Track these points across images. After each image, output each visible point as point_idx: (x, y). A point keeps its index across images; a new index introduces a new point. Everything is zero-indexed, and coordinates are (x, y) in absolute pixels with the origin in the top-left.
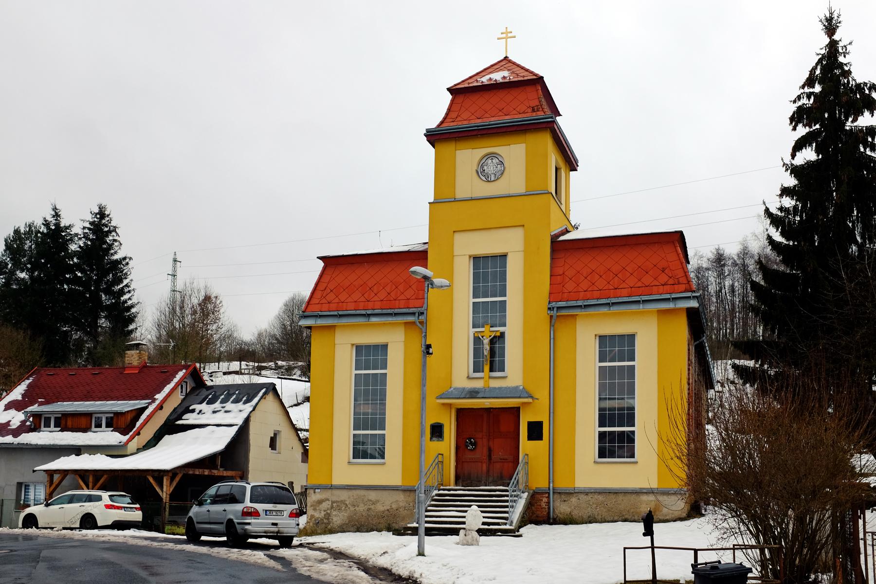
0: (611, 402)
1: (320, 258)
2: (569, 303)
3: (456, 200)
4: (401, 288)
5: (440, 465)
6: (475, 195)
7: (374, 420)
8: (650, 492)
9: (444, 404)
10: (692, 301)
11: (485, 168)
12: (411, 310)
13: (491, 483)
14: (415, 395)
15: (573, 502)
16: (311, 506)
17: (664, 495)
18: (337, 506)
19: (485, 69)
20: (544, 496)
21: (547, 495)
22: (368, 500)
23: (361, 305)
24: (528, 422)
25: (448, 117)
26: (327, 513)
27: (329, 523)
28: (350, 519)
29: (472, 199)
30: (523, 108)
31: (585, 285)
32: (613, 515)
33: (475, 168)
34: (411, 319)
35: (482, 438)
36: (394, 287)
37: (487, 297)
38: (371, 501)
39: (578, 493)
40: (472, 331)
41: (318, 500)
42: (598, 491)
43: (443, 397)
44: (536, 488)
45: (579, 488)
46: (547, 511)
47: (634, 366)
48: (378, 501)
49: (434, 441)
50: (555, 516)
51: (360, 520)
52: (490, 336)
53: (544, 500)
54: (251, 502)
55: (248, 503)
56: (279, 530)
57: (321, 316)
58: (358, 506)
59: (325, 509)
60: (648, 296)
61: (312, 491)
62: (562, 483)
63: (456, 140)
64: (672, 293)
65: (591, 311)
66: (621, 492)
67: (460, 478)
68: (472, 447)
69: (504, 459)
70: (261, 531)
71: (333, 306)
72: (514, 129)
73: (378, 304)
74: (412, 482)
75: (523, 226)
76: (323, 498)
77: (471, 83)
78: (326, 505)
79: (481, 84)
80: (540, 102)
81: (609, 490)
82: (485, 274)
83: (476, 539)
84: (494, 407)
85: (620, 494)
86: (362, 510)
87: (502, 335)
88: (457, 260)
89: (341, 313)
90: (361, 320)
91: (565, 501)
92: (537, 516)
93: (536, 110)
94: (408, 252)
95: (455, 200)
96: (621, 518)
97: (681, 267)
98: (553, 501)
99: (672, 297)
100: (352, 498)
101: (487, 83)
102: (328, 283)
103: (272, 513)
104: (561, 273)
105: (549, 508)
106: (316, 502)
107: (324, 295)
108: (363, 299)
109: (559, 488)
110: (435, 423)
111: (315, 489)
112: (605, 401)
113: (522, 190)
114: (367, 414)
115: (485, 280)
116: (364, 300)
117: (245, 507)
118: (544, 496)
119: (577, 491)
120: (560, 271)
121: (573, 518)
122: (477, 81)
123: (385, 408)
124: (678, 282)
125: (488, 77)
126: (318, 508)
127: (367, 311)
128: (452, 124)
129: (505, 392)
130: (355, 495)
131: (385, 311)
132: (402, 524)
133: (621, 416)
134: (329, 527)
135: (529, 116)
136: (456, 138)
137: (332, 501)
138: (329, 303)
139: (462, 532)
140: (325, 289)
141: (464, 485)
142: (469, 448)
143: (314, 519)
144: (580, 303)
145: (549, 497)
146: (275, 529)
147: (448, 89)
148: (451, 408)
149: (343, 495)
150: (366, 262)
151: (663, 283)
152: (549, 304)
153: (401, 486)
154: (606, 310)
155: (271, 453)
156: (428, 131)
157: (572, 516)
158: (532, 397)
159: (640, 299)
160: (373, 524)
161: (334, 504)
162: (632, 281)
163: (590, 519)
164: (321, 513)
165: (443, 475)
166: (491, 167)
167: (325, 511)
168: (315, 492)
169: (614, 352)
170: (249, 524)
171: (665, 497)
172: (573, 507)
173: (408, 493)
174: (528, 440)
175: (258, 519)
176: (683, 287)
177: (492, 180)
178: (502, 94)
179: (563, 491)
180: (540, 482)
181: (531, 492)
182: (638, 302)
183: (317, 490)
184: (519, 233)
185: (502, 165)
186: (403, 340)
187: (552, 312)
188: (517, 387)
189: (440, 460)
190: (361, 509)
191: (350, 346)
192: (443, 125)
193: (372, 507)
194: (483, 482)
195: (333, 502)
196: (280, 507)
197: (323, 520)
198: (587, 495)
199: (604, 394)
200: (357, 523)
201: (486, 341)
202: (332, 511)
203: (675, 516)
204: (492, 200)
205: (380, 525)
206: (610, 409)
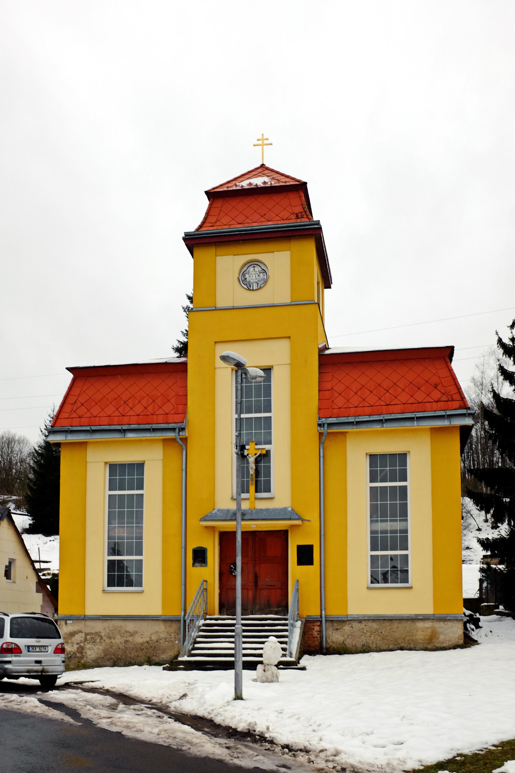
1: (70, 369)
2: (340, 419)
3: (217, 308)
4: (159, 402)
5: (205, 593)
6: (237, 304)
7: (130, 544)
8: (425, 618)
9: (206, 527)
10: (467, 418)
11: (247, 276)
12: (171, 426)
13: (257, 611)
14: (176, 517)
15: (346, 630)
17: (440, 621)
18: (92, 638)
19: (249, 172)
20: (316, 624)
21: (319, 624)
22: (125, 631)
23: (116, 419)
24: (297, 546)
25: (207, 221)
26: (81, 646)
27: (82, 657)
28: (106, 652)
29: (233, 308)
30: (285, 214)
31: (355, 400)
32: (388, 643)
33: (237, 276)
34: (170, 435)
35: (247, 564)
36: (151, 401)
38: (128, 632)
39: (351, 620)
41: (70, 633)
42: (372, 618)
43: (207, 519)
44: (307, 616)
45: (352, 615)
46: (319, 641)
47: (406, 486)
48: (136, 633)
49: (196, 566)
50: (328, 646)
51: (117, 653)
52: (255, 454)
53: (315, 629)
54: (12, 636)
55: (7, 637)
56: (43, 669)
57: (72, 432)
58: (114, 638)
59: (77, 642)
60: (422, 413)
61: (63, 623)
62: (333, 611)
63: (216, 246)
64: (446, 410)
65: (363, 428)
66: (396, 619)
67: (224, 607)
69: (271, 586)
70: (23, 670)
71: (84, 420)
72: (279, 235)
73: (134, 419)
74: (176, 611)
75: (289, 337)
76: (76, 630)
77: (230, 187)
78: (78, 638)
79: (241, 188)
80: (304, 209)
81: (383, 617)
83: (277, 675)
84: (260, 530)
85: (395, 622)
86: (119, 643)
87: (268, 452)
89: (93, 428)
90: (116, 436)
91: (337, 629)
92: (309, 646)
93: (300, 217)
94: (166, 364)
95: (216, 309)
96: (396, 646)
97: (454, 383)
98: (326, 630)
99: (448, 413)
101: (247, 187)
102: (79, 395)
103: (36, 649)
104: (329, 387)
105: (322, 638)
106: (68, 634)
107: (74, 409)
108: (117, 413)
109: (331, 615)
110: (198, 548)
111: (67, 620)
112: (377, 524)
113: (288, 301)
114: (122, 538)
115: (248, 395)
116: (119, 414)
117: (5, 643)
118: (316, 624)
119: (350, 619)
120: (328, 386)
121: (346, 647)
122: (236, 185)
123: (142, 531)
124: (452, 398)
125: (248, 182)
126: (69, 641)
127: (123, 426)
128: (211, 228)
129: (273, 513)
130: (110, 627)
131: (142, 427)
132: (163, 656)
133: (394, 539)
134: (83, 661)
135: (293, 222)
136: (216, 242)
137: (85, 633)
138: (80, 417)
139: (259, 667)
140: (75, 403)
141: (229, 613)
144: (351, 419)
145: (321, 626)
146: (38, 667)
147: (207, 193)
148: (214, 531)
149: (98, 627)
150: (120, 375)
151: (436, 400)
152: (319, 420)
153: (162, 616)
154: (379, 427)
155: (7, 582)
156: (187, 234)
157: (345, 645)
158: (300, 518)
159: (414, 416)
160: (131, 658)
161: (88, 637)
162: (404, 397)
163: (364, 648)
164: (73, 646)
165: (207, 604)
166: (253, 274)
167: (77, 644)
168: (66, 624)
169: (384, 472)
170: (9, 662)
171: (442, 624)
172: (346, 636)
173: (169, 624)
175: (20, 656)
176: (457, 404)
177: (254, 289)
178: (263, 200)
179: (336, 619)
180: (314, 611)
181: (304, 620)
182: (411, 419)
183: (68, 622)
184: (285, 345)
185: (265, 274)
186: (162, 458)
187: (322, 428)
188: (285, 509)
189: (205, 587)
191: (103, 463)
192: (203, 229)
193: (130, 639)
194: (249, 610)
195: (86, 634)
196: (44, 642)
197: (76, 654)
198: (360, 622)
199: (376, 516)
200: (113, 657)
201: (252, 460)
202: (86, 644)
203: (453, 643)
204: (255, 310)
205: (139, 658)
206: (382, 532)
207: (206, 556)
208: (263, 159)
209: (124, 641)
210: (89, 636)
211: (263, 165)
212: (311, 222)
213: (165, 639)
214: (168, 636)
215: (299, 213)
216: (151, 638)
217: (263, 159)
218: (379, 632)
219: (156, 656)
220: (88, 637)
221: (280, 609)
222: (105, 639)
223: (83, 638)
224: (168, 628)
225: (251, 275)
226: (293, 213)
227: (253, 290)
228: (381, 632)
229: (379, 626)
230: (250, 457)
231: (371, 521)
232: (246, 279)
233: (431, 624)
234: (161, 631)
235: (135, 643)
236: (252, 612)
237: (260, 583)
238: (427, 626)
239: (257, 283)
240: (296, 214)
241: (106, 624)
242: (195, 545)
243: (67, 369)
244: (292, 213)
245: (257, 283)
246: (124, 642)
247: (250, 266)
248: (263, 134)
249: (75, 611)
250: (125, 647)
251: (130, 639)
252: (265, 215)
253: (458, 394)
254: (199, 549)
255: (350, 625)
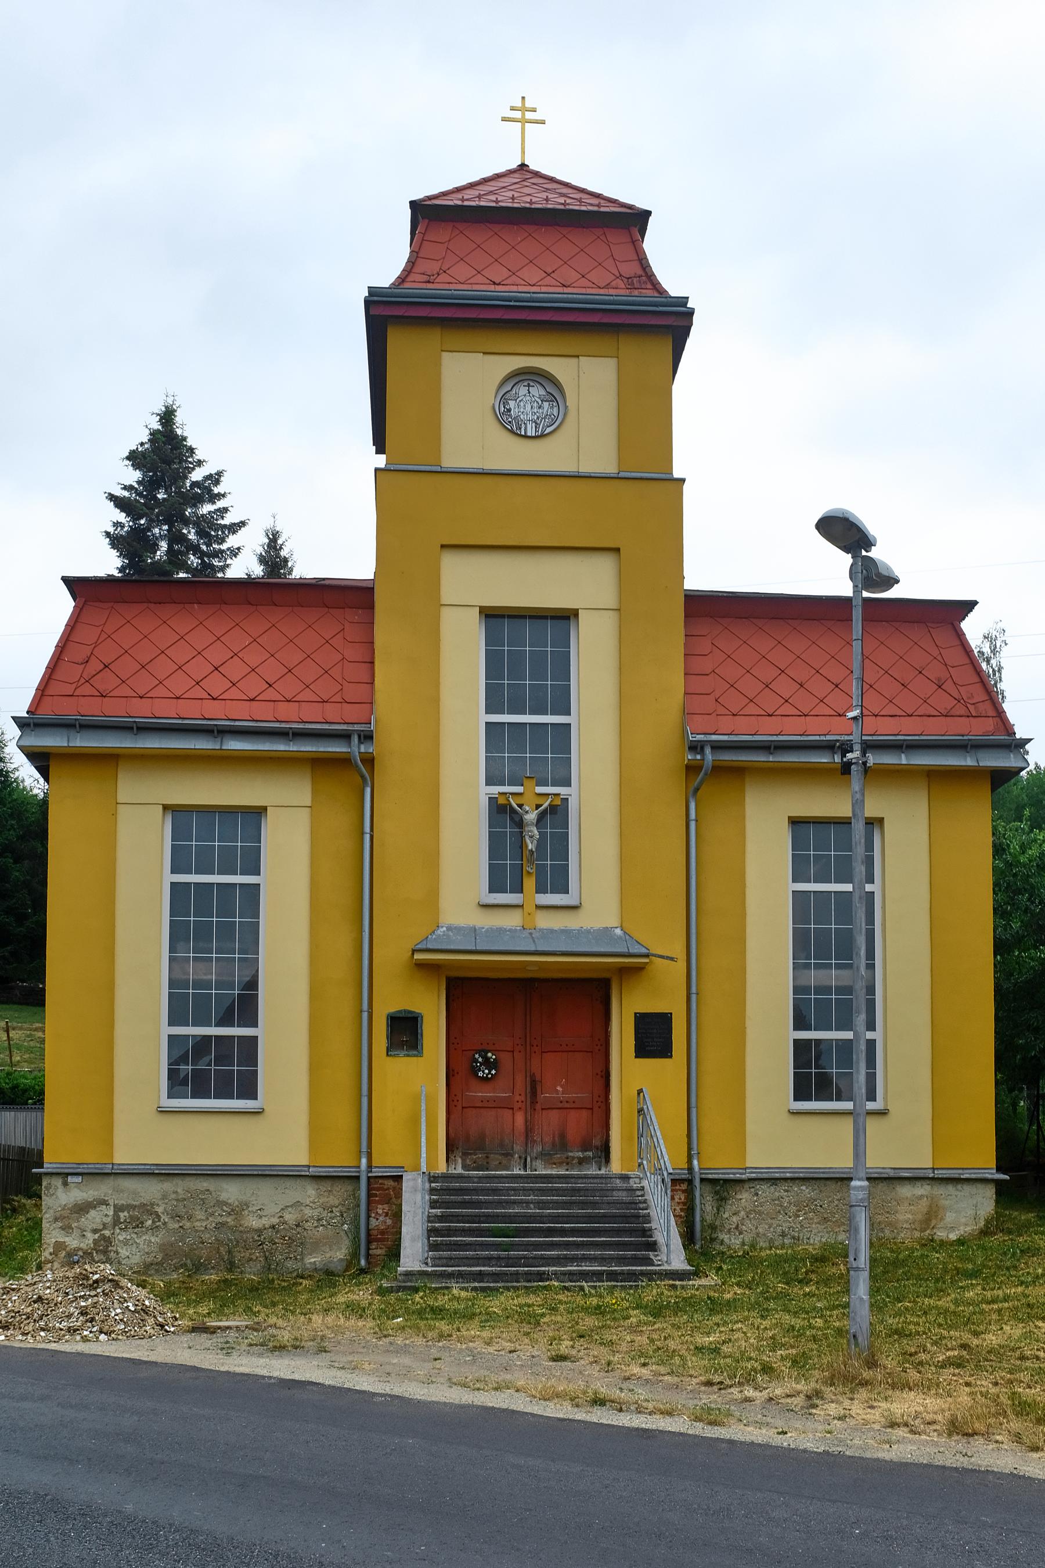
0: (822, 972)
1: (69, 582)
3: (443, 470)
8: (915, 1179)
11: (512, 404)
16: (56, 1219)
17: (947, 1184)
18: (131, 1217)
21: (684, 1187)
26: (104, 1238)
37: (523, 712)
38: (226, 1204)
40: (486, 792)
61: (57, 1182)
68: (489, 1073)
75: (618, 550)
82: (517, 659)
88: (449, 619)
100: (173, 1196)
110: (400, 1012)
113: (611, 469)
115: (516, 673)
132: (313, 1260)
137: (115, 1206)
141: (468, 1162)
142: (480, 1074)
143: (64, 1253)
149: (150, 1191)
153: (309, 1166)
161: (122, 1215)
172: (743, 1213)
173: (327, 1185)
174: (636, 1057)
183: (70, 1179)
190: (198, 1224)
195: (118, 1209)
197: (91, 1254)
207: (419, 1031)
208: (523, 152)
209: (214, 1225)
210: (126, 1213)
211: (523, 166)
212: (663, 299)
213: (319, 1220)
214: (325, 1213)
215: (635, 277)
216: (281, 1217)
217: (523, 152)
218: (816, 1205)
219: (296, 1259)
220: (123, 1215)
221: (590, 1154)
222: (166, 1220)
223: (111, 1217)
224: (326, 1194)
225: (522, 404)
226: (621, 275)
227: (526, 437)
228: (821, 1206)
229: (815, 1192)
230: (527, 812)
231: (796, 967)
232: (509, 410)
233: (928, 1188)
234: (308, 1203)
235: (241, 1229)
236: (523, 1161)
237: (544, 1096)
238: (920, 1194)
239: (536, 423)
240: (628, 278)
241: (168, 1186)
242: (395, 1006)
243: (66, 580)
244: (618, 275)
245: (536, 423)
246: (215, 1228)
247: (520, 384)
248: (523, 98)
249: (89, 1156)
250: (216, 1240)
251: (229, 1220)
252: (554, 272)
253: (988, 704)
254: (403, 1015)
255: (753, 1190)
